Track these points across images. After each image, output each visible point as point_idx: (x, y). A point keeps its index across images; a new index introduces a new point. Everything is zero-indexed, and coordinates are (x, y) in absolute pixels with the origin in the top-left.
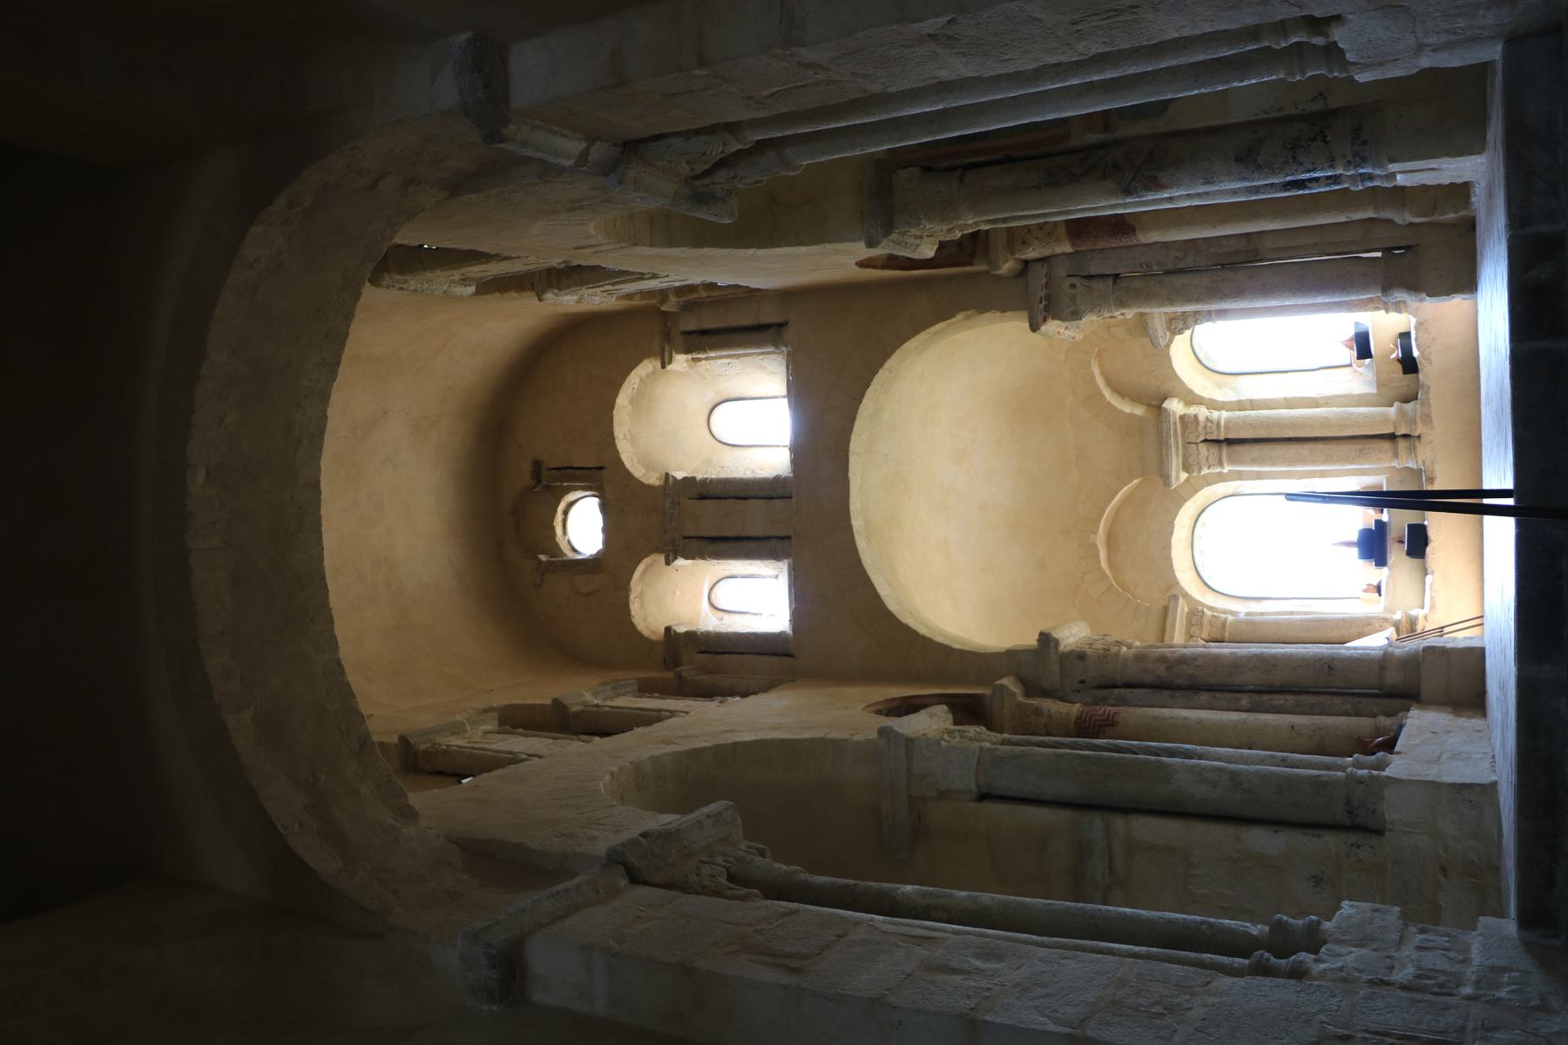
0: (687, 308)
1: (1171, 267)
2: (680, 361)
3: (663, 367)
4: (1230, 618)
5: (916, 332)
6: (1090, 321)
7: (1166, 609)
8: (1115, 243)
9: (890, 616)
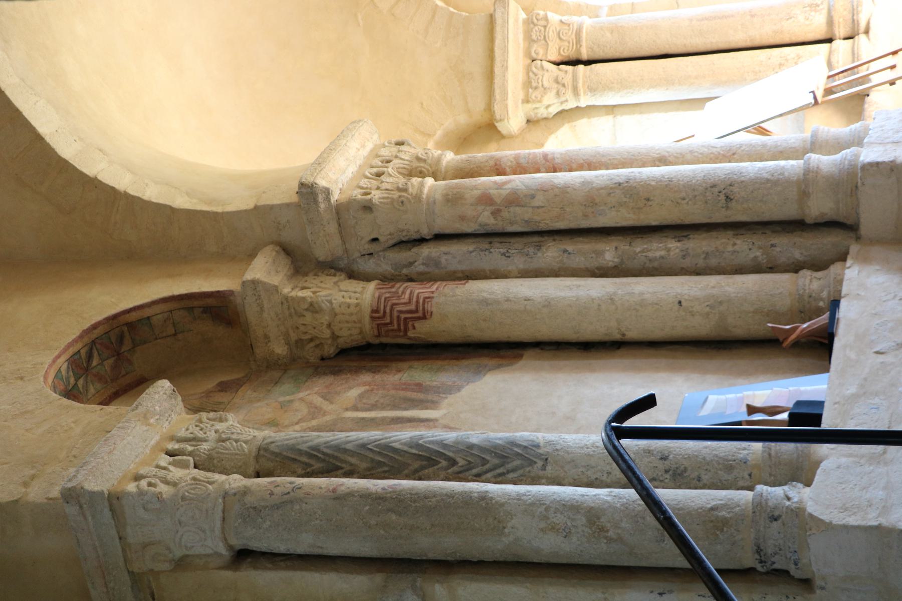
4: (587, 22)
7: (492, 19)
9: (64, 166)
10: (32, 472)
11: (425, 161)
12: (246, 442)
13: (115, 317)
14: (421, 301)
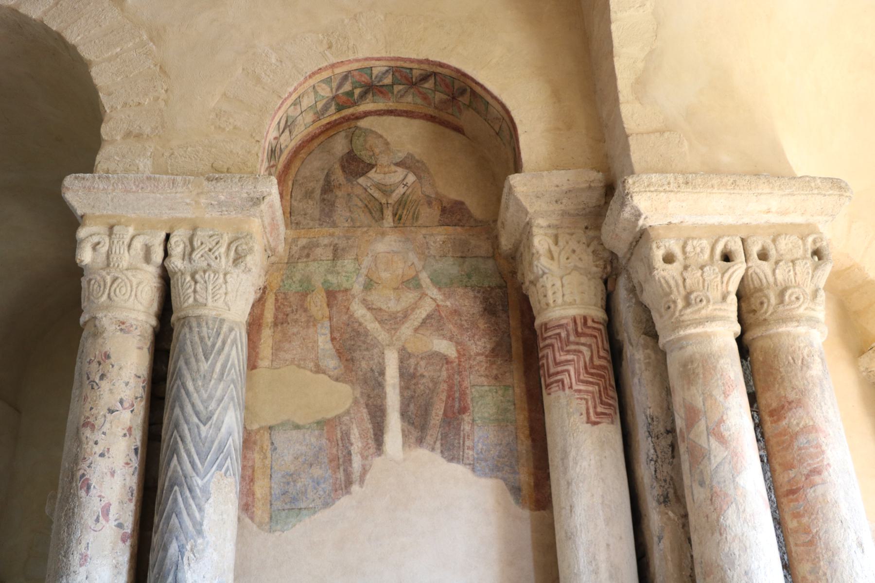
10: (147, 130)
11: (782, 302)
12: (195, 300)
13: (465, 75)
14: (559, 377)
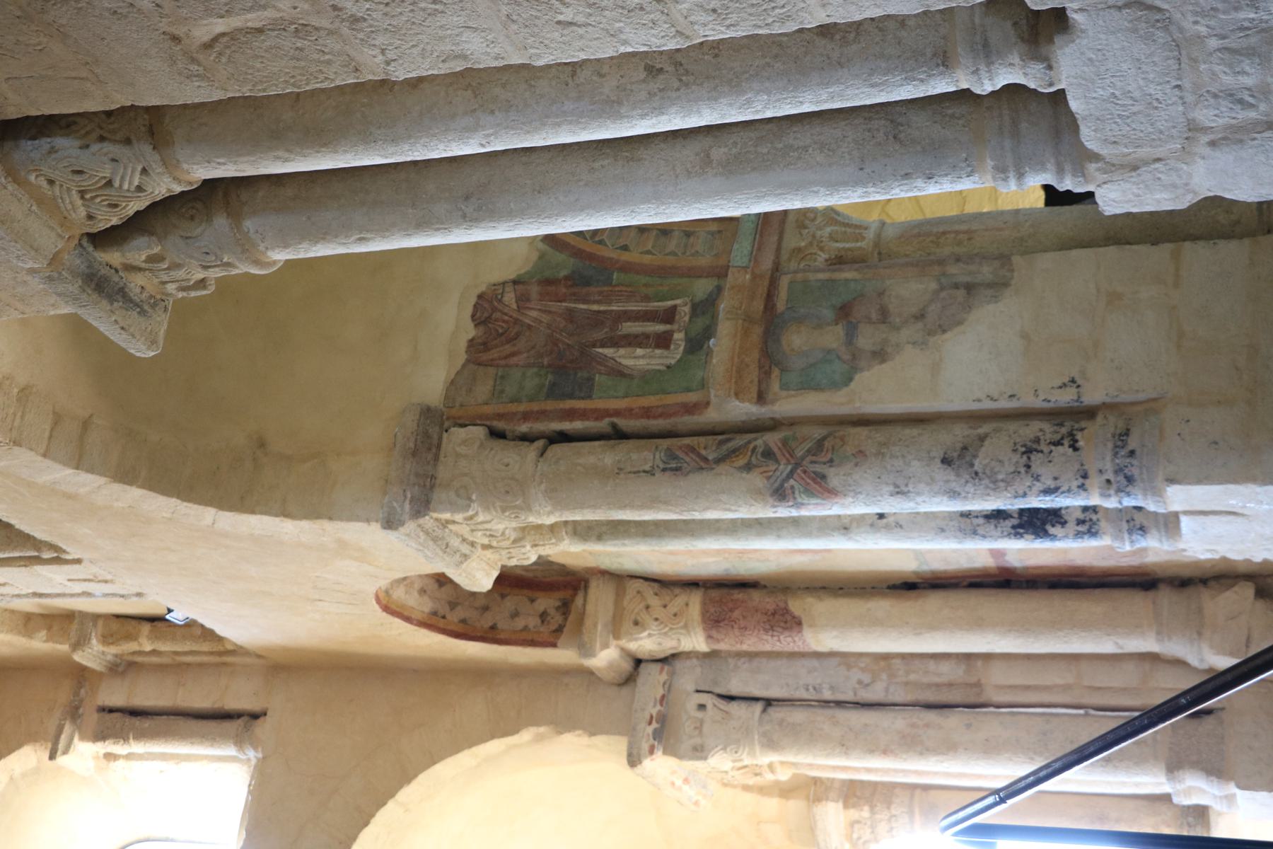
0: (123, 668)
1: (849, 696)
2: (84, 754)
3: (52, 756)
5: (455, 747)
6: (720, 761)
8: (770, 643)
